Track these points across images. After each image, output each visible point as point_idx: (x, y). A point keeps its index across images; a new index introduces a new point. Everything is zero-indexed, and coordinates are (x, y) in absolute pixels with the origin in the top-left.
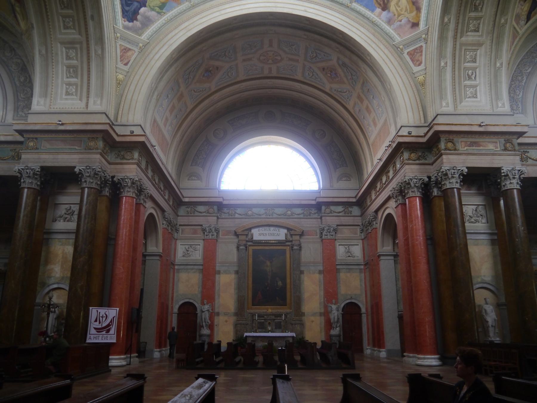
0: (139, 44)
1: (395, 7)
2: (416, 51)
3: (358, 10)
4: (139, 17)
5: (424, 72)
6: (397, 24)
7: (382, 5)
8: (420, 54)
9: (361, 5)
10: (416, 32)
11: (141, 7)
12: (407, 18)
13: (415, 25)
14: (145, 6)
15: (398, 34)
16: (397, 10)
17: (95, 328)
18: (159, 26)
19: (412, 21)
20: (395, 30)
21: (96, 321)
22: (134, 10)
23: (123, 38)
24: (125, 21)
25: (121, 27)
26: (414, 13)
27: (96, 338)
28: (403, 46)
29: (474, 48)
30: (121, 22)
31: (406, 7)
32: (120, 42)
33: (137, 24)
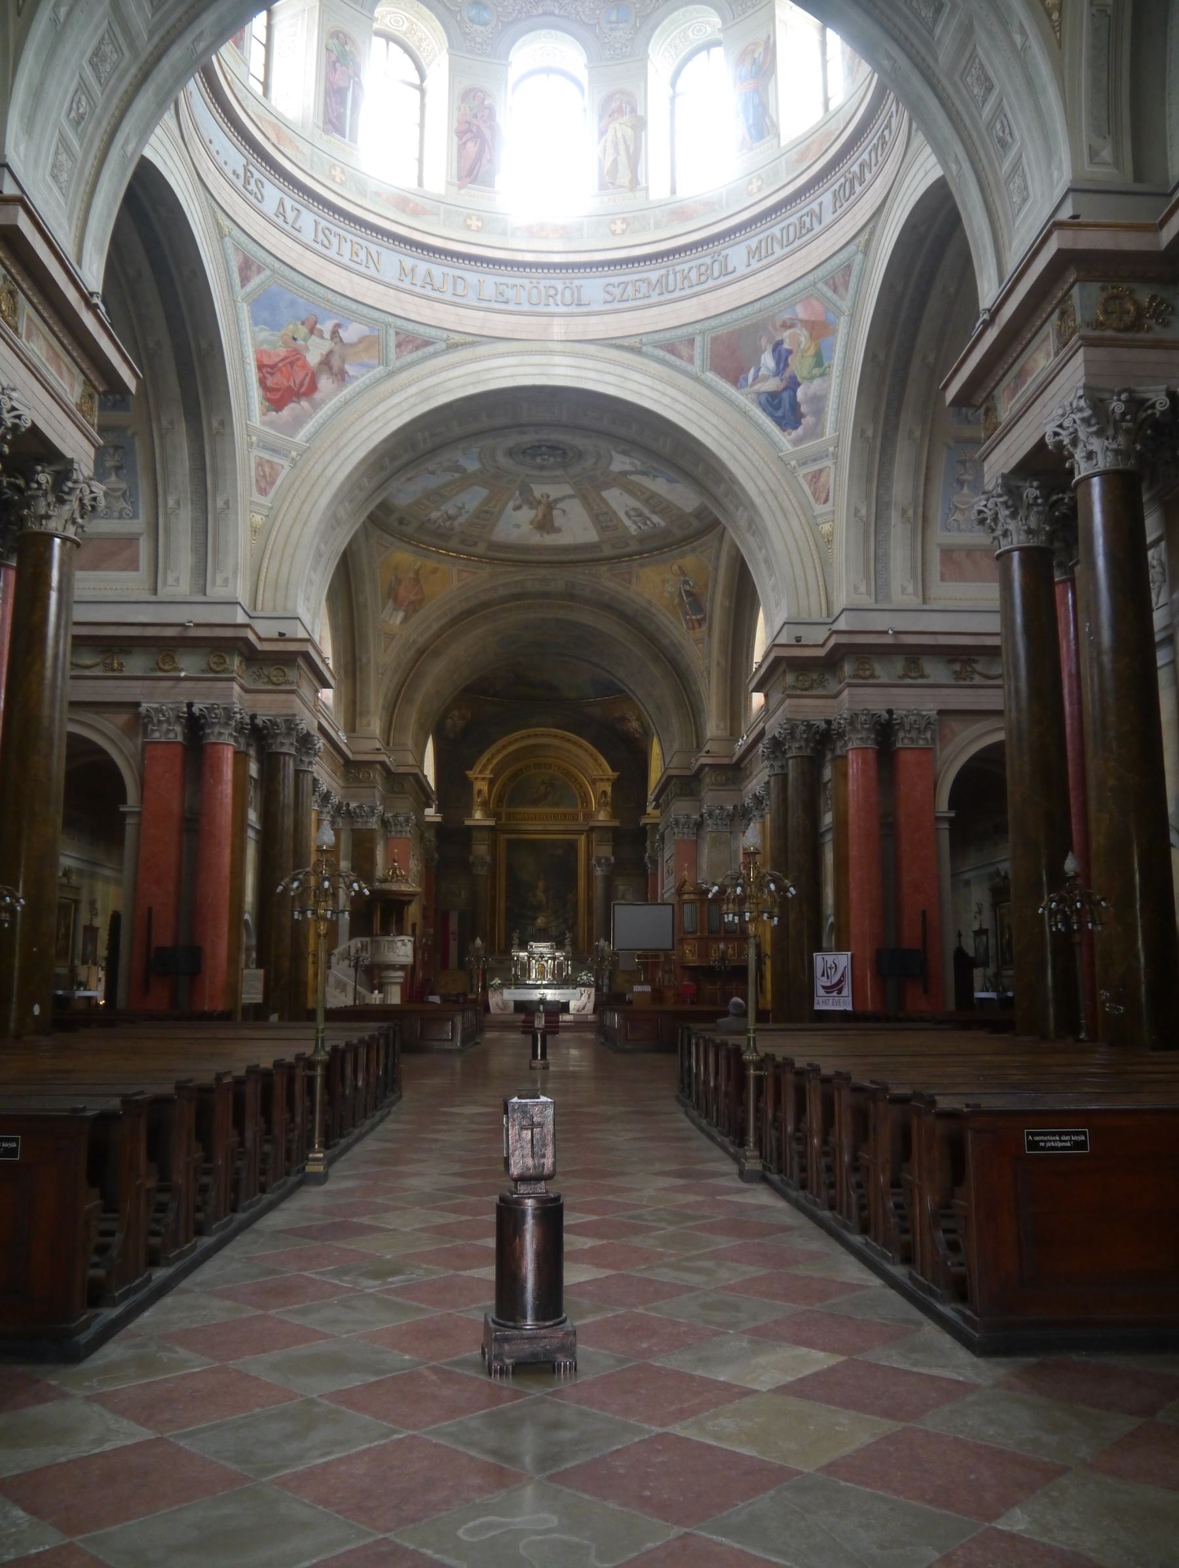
0: (827, 450)
4: (803, 409)
11: (795, 392)
14: (799, 385)
17: (824, 987)
18: (836, 394)
21: (823, 975)
22: (790, 404)
23: (803, 463)
24: (790, 434)
25: (789, 446)
27: (824, 1002)
29: (967, 54)
30: (784, 440)
32: (802, 472)
33: (808, 420)
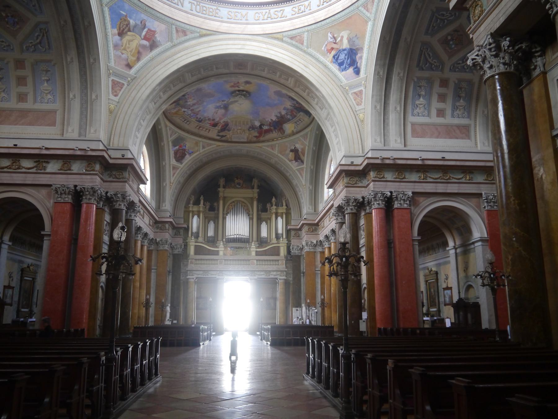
1: (127, 42)
2: (119, 84)
3: (105, 15)
5: (116, 104)
6: (119, 53)
7: (121, 31)
8: (120, 88)
9: (110, 14)
10: (125, 71)
12: (128, 56)
13: (129, 66)
15: (115, 60)
16: (126, 44)
19: (129, 62)
20: (115, 55)
26: (134, 59)
28: (113, 72)
31: (132, 49)
